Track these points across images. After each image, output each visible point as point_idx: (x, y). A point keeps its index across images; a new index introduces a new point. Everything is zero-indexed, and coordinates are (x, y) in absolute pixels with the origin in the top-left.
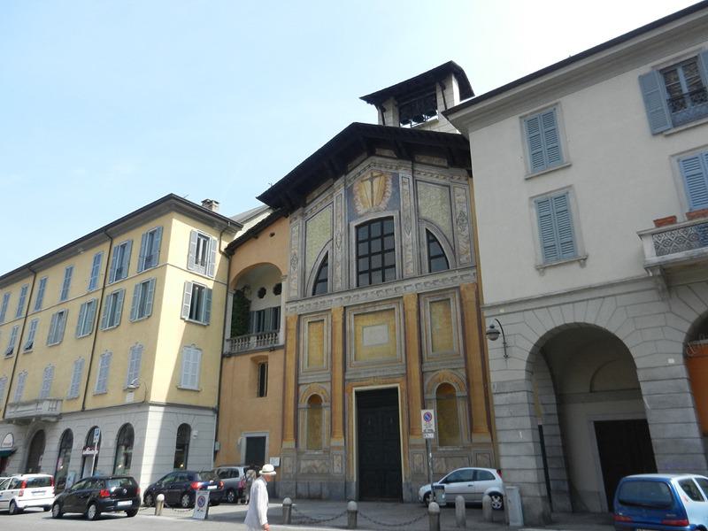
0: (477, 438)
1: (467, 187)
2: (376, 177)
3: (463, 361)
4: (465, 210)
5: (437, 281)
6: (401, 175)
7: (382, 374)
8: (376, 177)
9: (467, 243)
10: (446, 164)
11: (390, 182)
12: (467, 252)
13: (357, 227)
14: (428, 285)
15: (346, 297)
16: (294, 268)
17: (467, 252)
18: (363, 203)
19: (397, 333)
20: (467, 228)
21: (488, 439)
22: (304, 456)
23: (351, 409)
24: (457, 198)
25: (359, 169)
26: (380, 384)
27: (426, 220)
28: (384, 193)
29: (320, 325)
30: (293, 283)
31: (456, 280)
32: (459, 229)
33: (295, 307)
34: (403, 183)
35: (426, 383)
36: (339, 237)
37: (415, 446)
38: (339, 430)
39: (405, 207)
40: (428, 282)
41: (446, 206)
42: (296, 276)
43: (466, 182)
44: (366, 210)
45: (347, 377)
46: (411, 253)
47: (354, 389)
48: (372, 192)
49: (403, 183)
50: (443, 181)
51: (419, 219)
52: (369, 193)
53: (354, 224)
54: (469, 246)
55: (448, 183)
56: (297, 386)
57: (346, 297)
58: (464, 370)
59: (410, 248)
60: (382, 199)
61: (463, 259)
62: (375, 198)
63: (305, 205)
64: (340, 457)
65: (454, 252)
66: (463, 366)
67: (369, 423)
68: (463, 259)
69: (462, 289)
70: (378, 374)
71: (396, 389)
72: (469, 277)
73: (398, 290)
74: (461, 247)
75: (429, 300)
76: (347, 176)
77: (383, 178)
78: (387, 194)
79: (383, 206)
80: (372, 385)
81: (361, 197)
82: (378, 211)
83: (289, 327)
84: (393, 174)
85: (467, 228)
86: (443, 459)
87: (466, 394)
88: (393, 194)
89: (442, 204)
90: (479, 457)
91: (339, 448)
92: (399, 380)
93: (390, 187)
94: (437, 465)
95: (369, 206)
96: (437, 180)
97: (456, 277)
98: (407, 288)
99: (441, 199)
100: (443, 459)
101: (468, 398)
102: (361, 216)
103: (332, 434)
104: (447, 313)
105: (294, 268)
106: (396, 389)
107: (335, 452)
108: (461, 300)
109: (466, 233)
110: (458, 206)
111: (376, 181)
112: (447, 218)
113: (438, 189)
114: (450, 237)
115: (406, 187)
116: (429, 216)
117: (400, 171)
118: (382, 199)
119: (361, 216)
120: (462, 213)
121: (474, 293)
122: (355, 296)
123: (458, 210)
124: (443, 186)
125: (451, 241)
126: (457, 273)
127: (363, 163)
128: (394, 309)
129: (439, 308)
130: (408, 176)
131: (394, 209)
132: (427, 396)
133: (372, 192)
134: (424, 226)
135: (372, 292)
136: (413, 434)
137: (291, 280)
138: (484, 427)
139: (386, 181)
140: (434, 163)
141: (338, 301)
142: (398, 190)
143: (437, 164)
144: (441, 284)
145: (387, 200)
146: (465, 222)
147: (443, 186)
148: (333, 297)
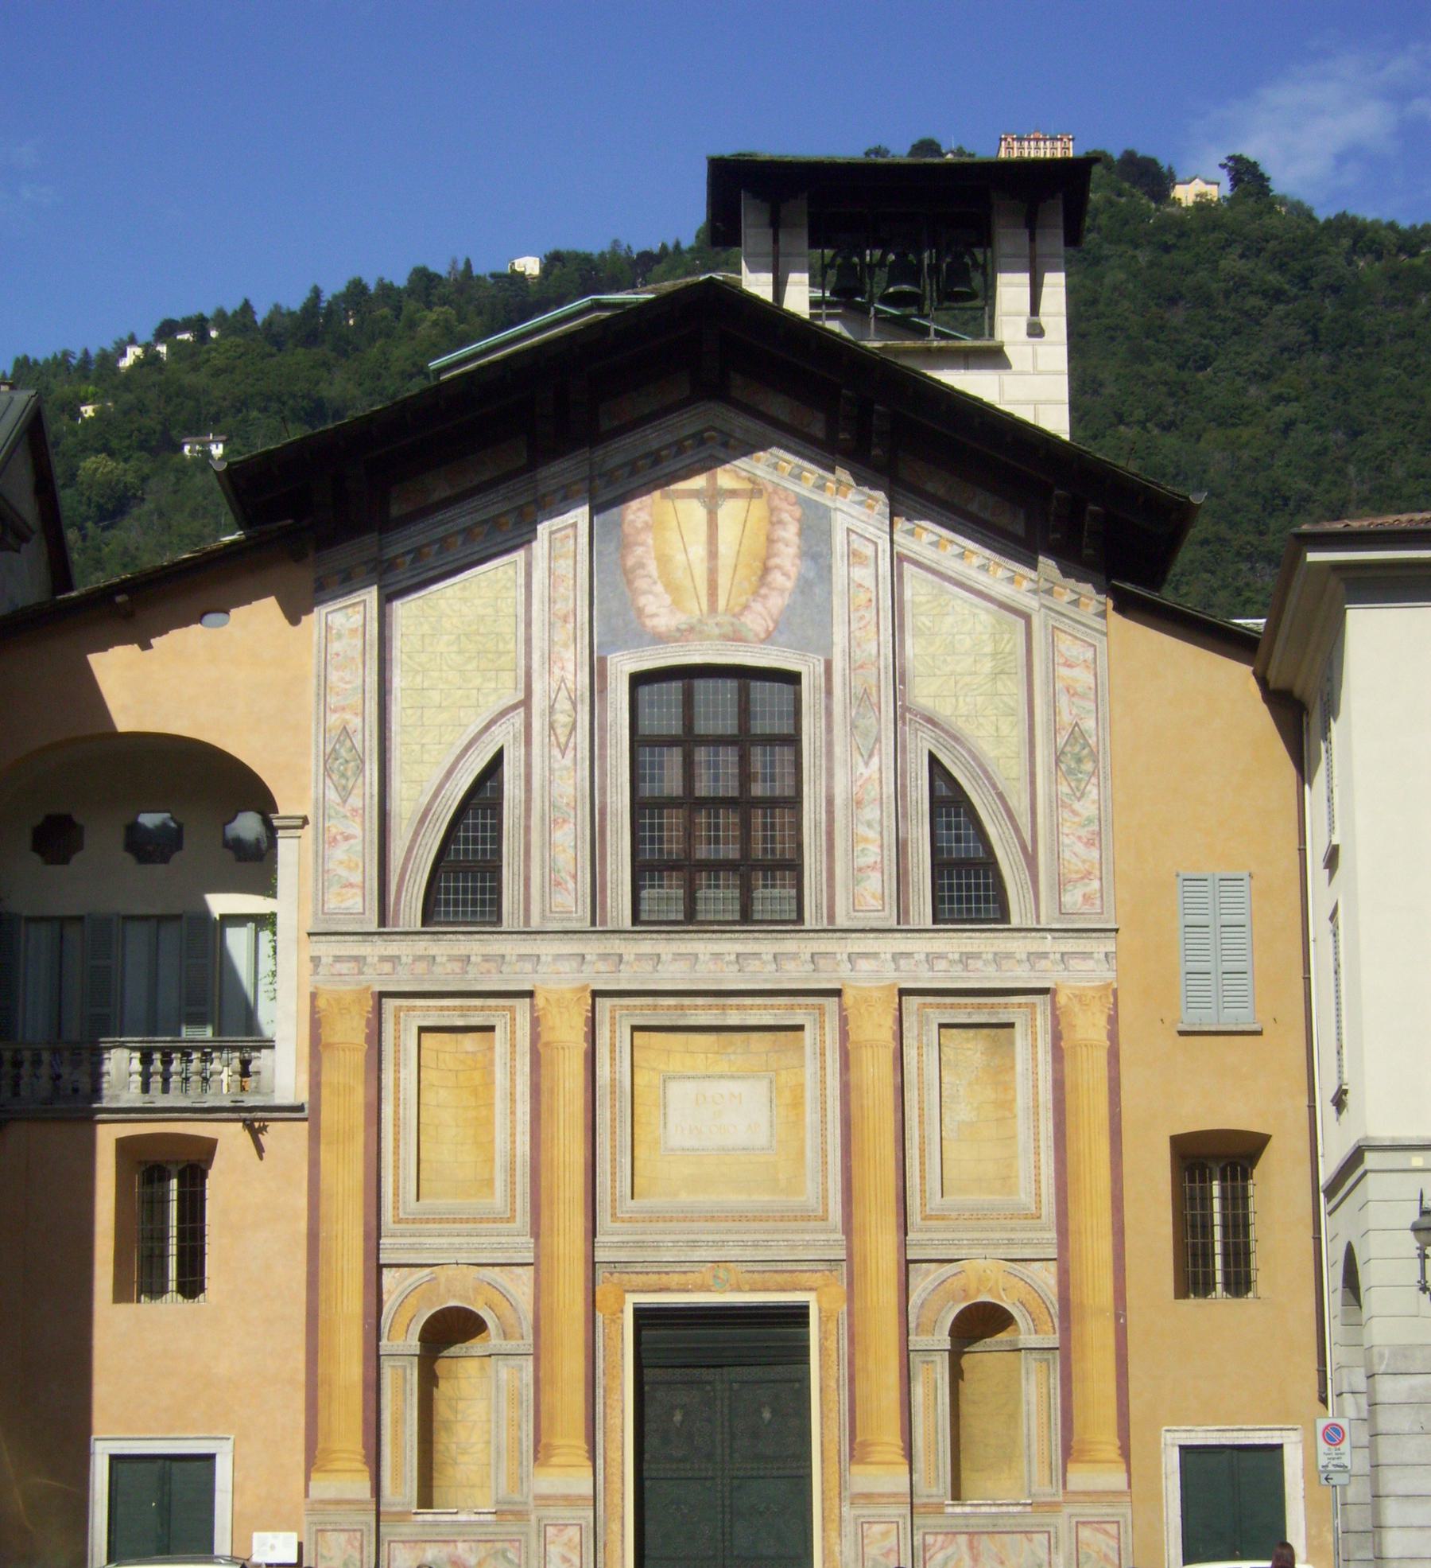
0: (1081, 1477)
1: (1101, 644)
2: (733, 493)
3: (1052, 1235)
4: (1089, 724)
5: (976, 956)
6: (840, 523)
7: (749, 1254)
8: (733, 493)
9: (1089, 843)
10: (1019, 528)
11: (790, 532)
12: (1087, 875)
13: (638, 680)
14: (941, 965)
15: (604, 957)
16: (345, 794)
17: (1087, 875)
18: (671, 587)
19: (811, 1117)
20: (1093, 792)
21: (1115, 1479)
22: (406, 1530)
23: (614, 1371)
24: (1062, 671)
25: (653, 438)
26: (738, 1289)
27: (930, 721)
28: (766, 570)
29: (469, 1041)
30: (339, 853)
31: (1043, 964)
32: (1064, 788)
33: (359, 960)
34: (853, 556)
35: (915, 1299)
36: (563, 704)
37: (868, 1497)
38: (569, 1437)
39: (858, 655)
40: (940, 956)
41: (1013, 688)
42: (355, 829)
43: (1098, 623)
44: (678, 620)
45: (600, 1255)
46: (873, 834)
47: (632, 1300)
48: (713, 554)
49: (853, 556)
50: (1003, 591)
51: (902, 711)
52: (698, 551)
53: (623, 665)
54: (1095, 854)
55: (1030, 603)
56: (376, 1270)
57: (604, 957)
58: (1053, 1267)
59: (871, 813)
60: (756, 593)
61: (1073, 898)
62: (724, 580)
63: (386, 525)
64: (573, 1533)
65: (1031, 860)
66: (1052, 1252)
67: (678, 1417)
68: (1073, 898)
69: (1062, 999)
70: (735, 1253)
71: (798, 1315)
72: (1090, 964)
73: (822, 963)
74: (1066, 855)
75: (938, 1017)
76: (599, 453)
77: (758, 507)
78: (777, 578)
79: (756, 621)
80: (708, 1289)
81: (663, 561)
82: (736, 637)
83: (327, 1036)
84: (802, 502)
85: (1093, 792)
86: (963, 1539)
87: (1053, 1340)
88: (804, 587)
89: (996, 675)
90: (1085, 1533)
91: (569, 1500)
92: (817, 1279)
93: (792, 551)
94: (940, 1557)
95: (695, 607)
96: (982, 580)
97: (1044, 955)
98: (864, 965)
99: (994, 655)
100: (963, 1539)
101: (1065, 1354)
102: (659, 639)
103: (541, 1451)
104: (1001, 1072)
105: (345, 794)
106: (798, 1315)
107: (552, 1512)
108: (1057, 1038)
109: (1087, 808)
110: (1063, 701)
111: (730, 511)
112: (1015, 735)
113: (985, 616)
114: (1019, 803)
115: (864, 575)
116: (944, 710)
117: (840, 503)
118: (756, 593)
119: (659, 639)
120: (1077, 733)
121: (1102, 1021)
122: (639, 957)
123: (1066, 718)
124: (1003, 605)
125: (1024, 822)
126: (1048, 943)
127: (672, 419)
128: (800, 1028)
129: (970, 1050)
130: (871, 531)
131: (803, 646)
132: (916, 1341)
133: (713, 554)
134: (921, 744)
135: (717, 956)
136: (862, 1462)
137: (325, 842)
138: (1111, 1450)
139: (773, 521)
140: (973, 507)
141: (566, 966)
142: (825, 572)
143: (986, 515)
144: (991, 970)
145: (776, 602)
146: (1088, 766)
147: (1003, 605)
148: (547, 948)
